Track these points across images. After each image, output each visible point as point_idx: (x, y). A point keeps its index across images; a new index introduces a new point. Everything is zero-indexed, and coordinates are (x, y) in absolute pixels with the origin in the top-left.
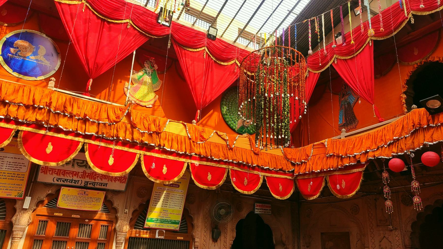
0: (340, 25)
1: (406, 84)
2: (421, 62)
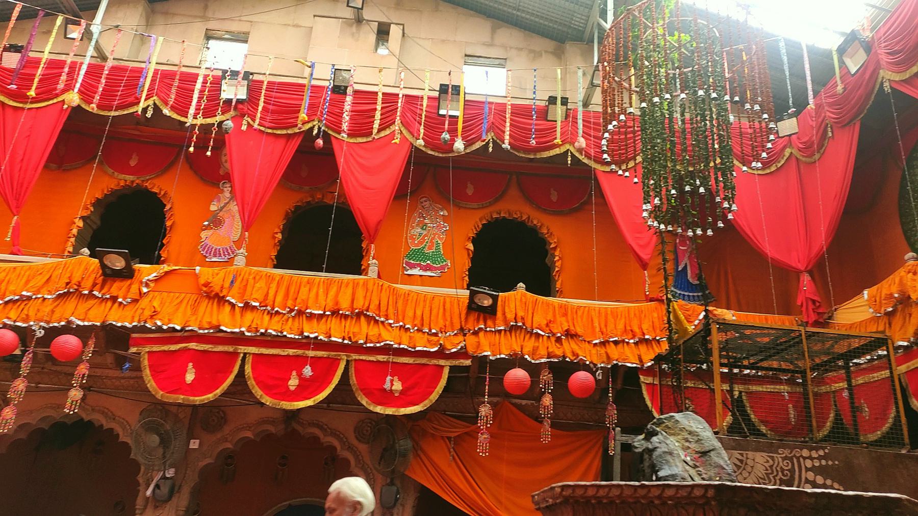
0: (28, 24)
1: (93, 205)
2: (132, 182)
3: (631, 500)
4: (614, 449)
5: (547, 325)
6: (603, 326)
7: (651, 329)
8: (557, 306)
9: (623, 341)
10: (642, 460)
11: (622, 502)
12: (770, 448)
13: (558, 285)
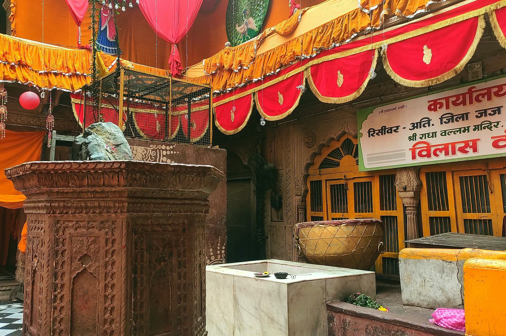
3: (76, 171)
4: (51, 144)
5: (4, 55)
6: (47, 62)
7: (81, 68)
8: (12, 42)
9: (61, 74)
10: (81, 150)
11: (70, 173)
12: (146, 144)
13: (13, 26)
